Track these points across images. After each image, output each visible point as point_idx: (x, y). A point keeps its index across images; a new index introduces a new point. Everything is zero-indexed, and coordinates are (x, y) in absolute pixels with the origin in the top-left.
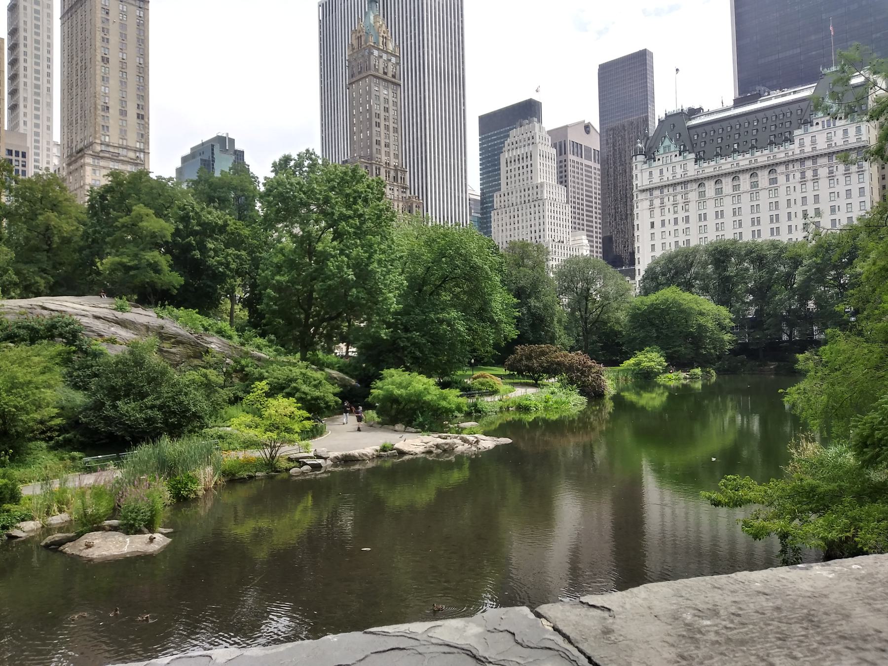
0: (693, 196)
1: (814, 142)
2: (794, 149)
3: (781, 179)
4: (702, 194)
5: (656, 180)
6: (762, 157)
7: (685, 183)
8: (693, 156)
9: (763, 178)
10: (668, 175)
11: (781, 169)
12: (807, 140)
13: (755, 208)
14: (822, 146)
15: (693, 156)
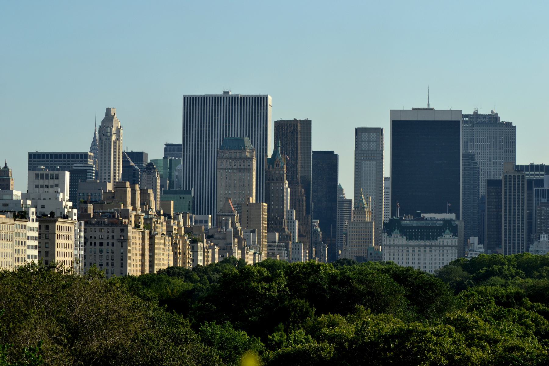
0: (405, 251)
1: (443, 242)
2: (437, 243)
3: (433, 251)
4: (408, 251)
5: (392, 243)
6: (428, 243)
7: (403, 246)
8: (405, 237)
9: (428, 249)
10: (396, 242)
11: (433, 248)
12: (441, 241)
13: (425, 259)
14: (445, 244)
15: (405, 237)
